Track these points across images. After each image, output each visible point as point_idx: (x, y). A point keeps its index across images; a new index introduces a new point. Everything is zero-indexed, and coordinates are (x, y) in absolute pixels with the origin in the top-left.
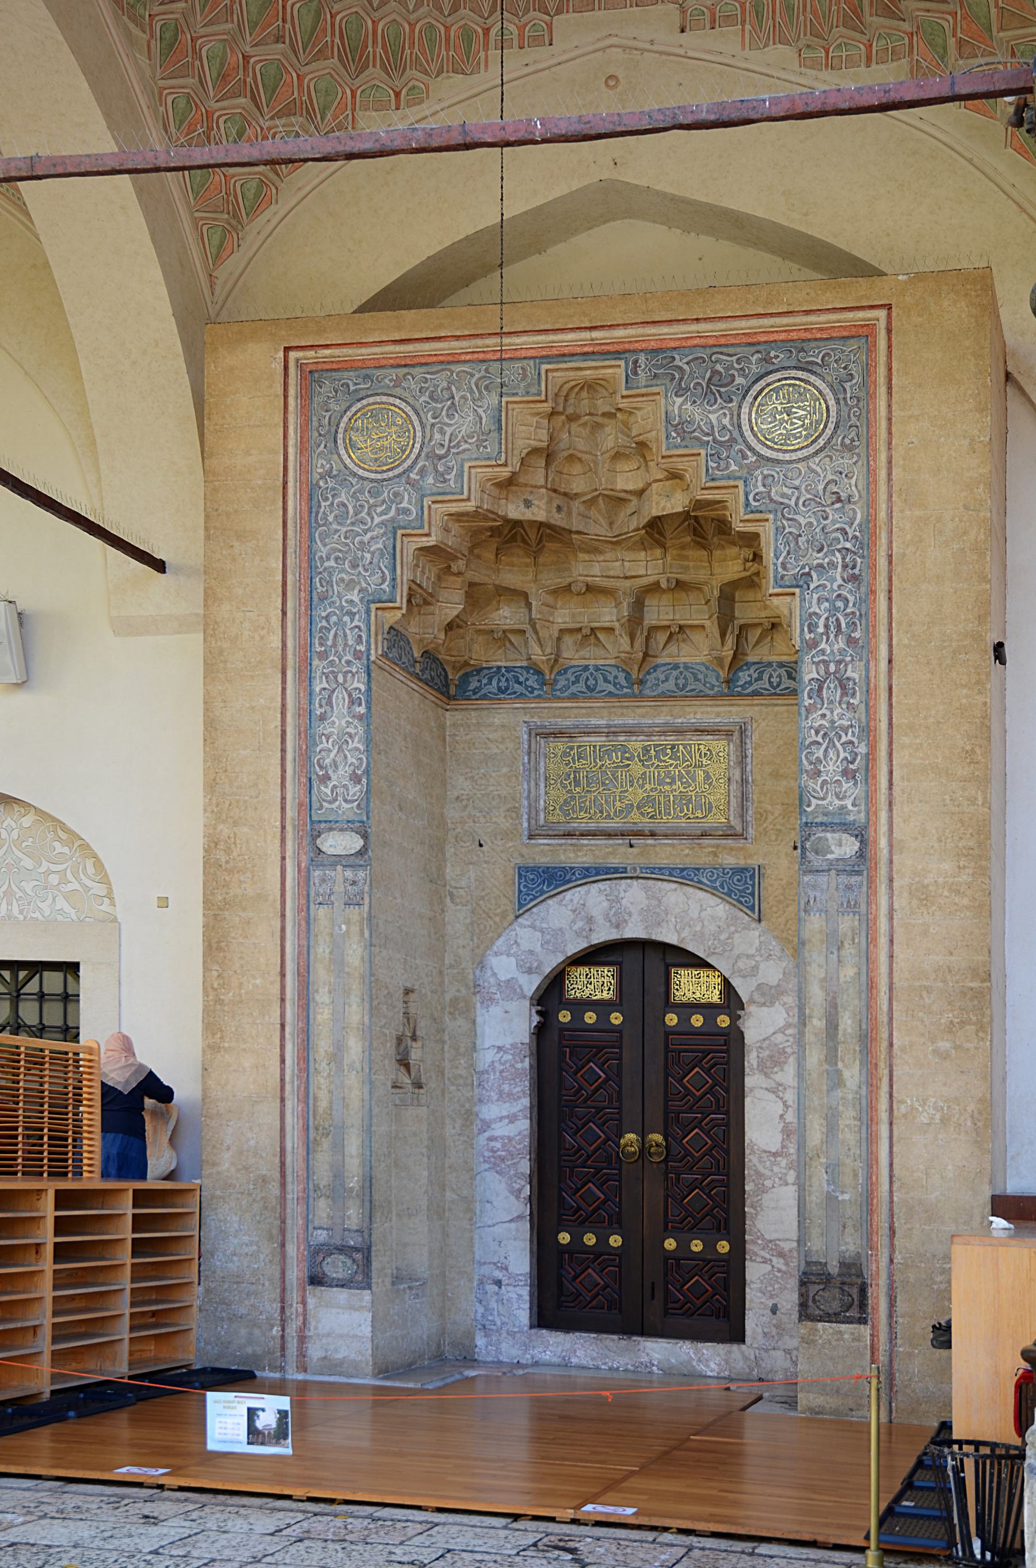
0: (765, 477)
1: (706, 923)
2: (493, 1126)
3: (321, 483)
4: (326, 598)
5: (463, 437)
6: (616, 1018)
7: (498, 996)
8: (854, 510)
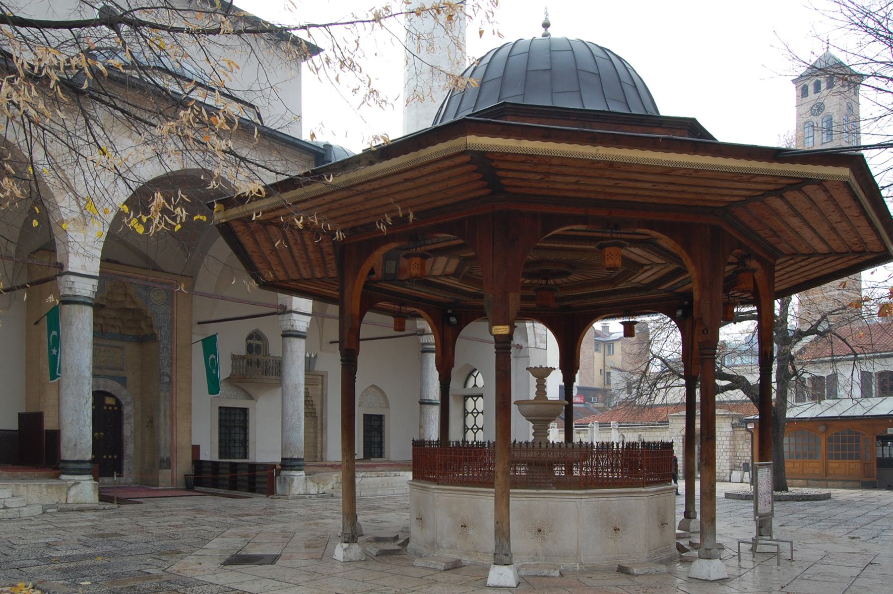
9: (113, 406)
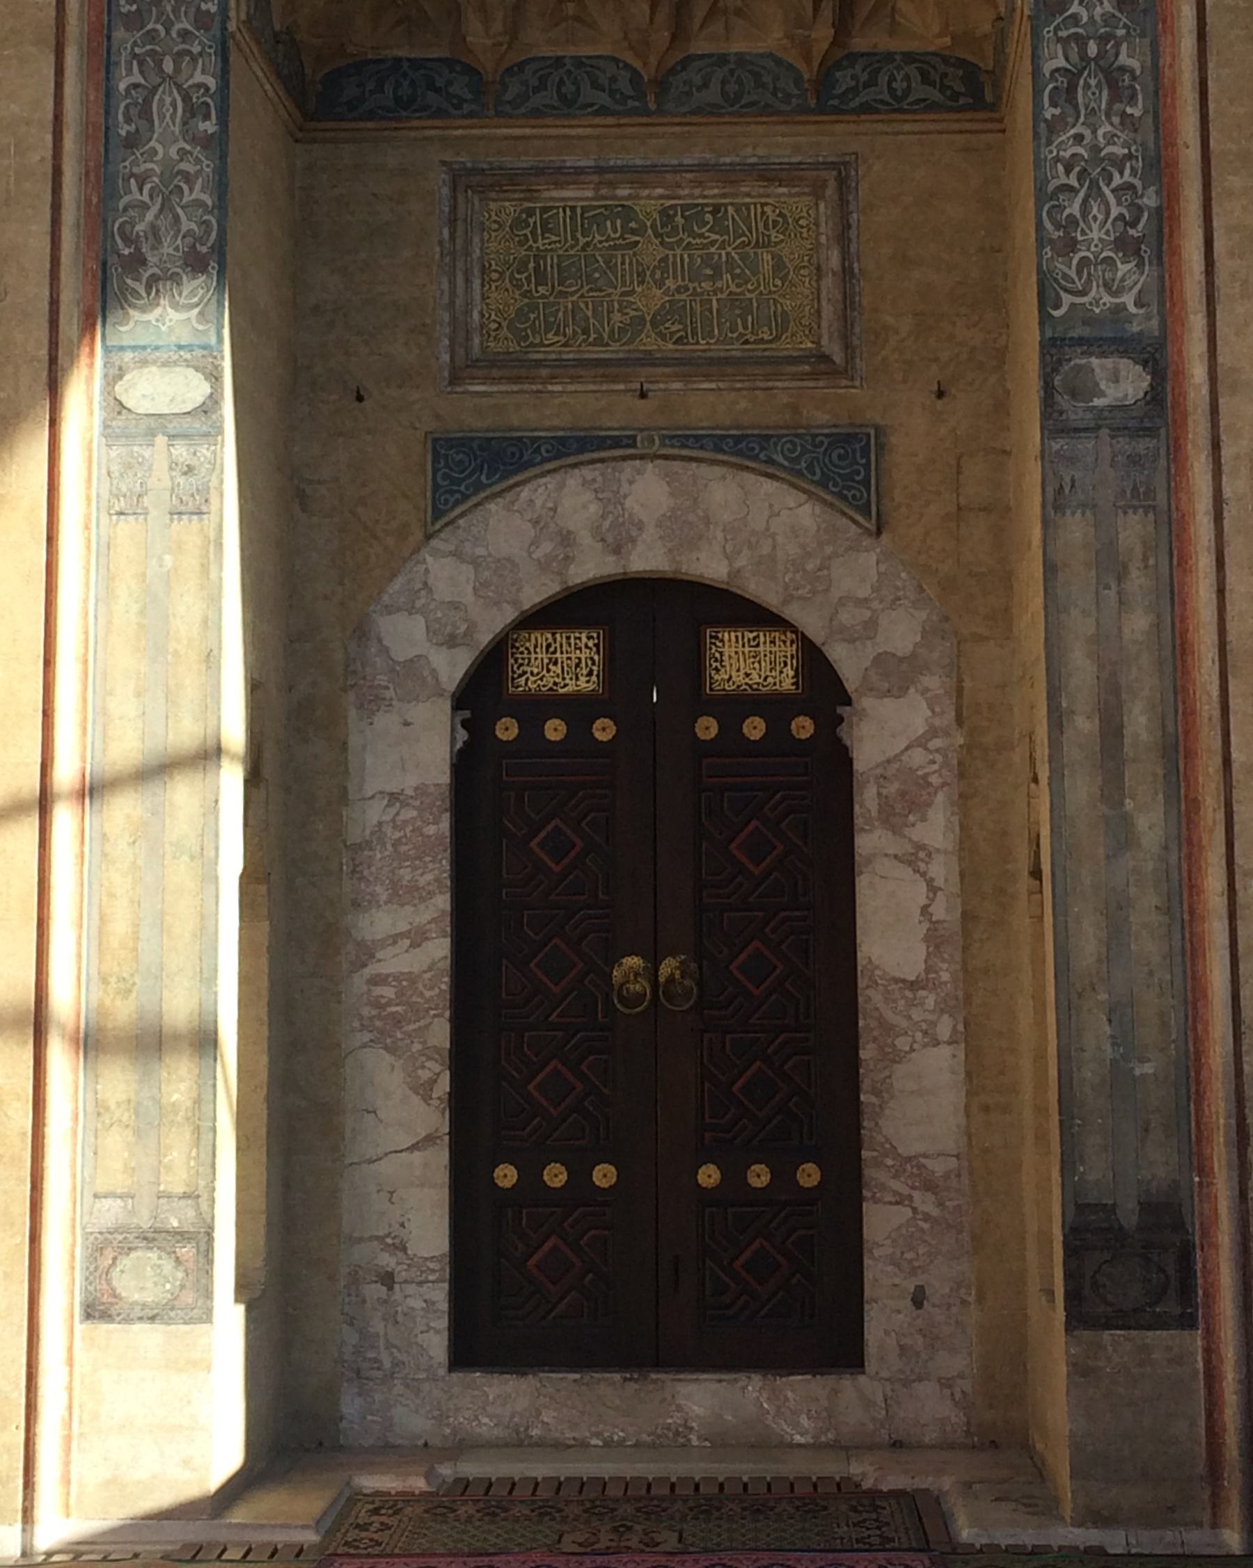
1: (780, 539)
2: (379, 955)
6: (603, 730)
7: (390, 693)
9: (774, 707)
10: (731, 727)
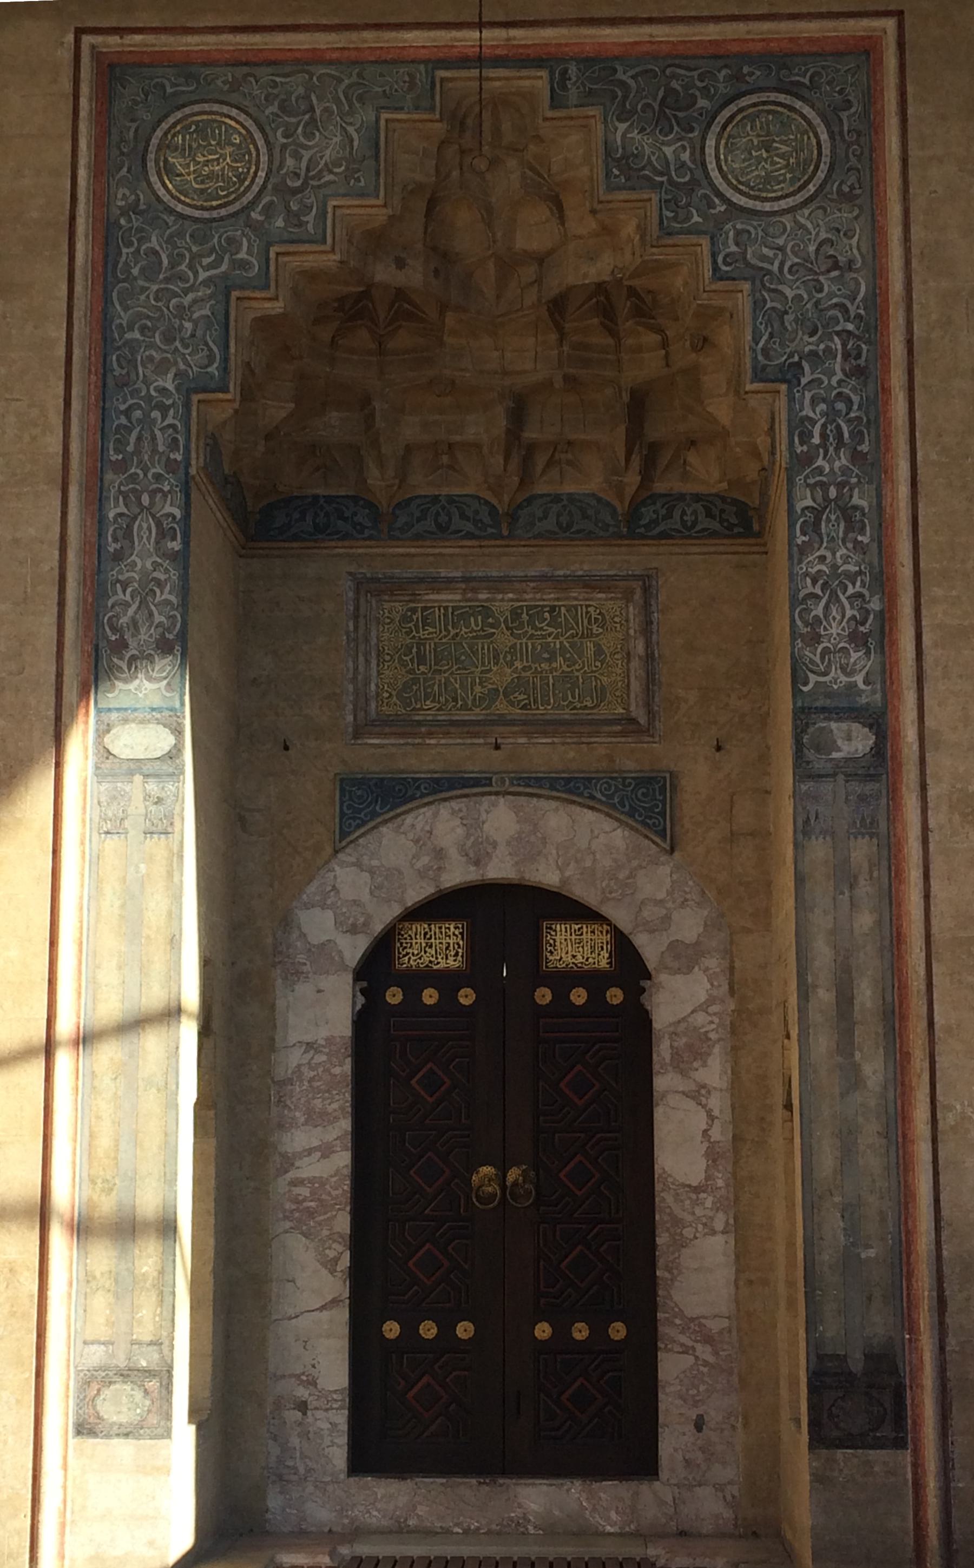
0: (738, 233)
1: (598, 857)
2: (297, 1164)
3: (122, 222)
4: (126, 385)
5: (326, 164)
7: (307, 968)
8: (856, 279)
10: (561, 996)
